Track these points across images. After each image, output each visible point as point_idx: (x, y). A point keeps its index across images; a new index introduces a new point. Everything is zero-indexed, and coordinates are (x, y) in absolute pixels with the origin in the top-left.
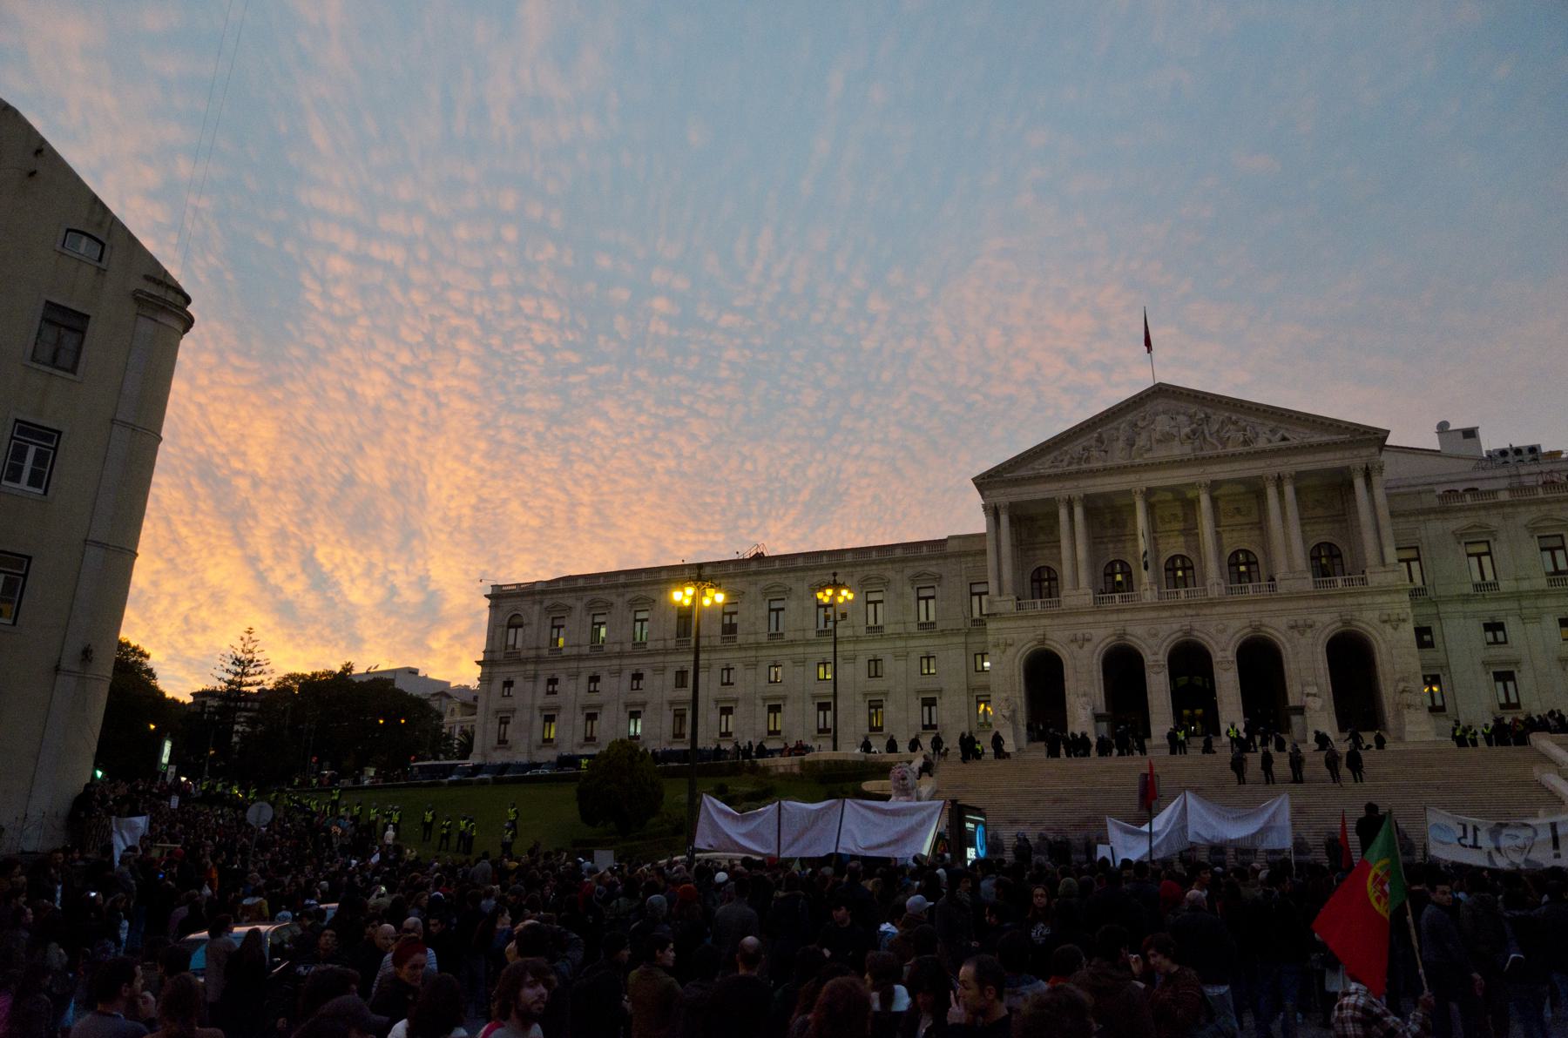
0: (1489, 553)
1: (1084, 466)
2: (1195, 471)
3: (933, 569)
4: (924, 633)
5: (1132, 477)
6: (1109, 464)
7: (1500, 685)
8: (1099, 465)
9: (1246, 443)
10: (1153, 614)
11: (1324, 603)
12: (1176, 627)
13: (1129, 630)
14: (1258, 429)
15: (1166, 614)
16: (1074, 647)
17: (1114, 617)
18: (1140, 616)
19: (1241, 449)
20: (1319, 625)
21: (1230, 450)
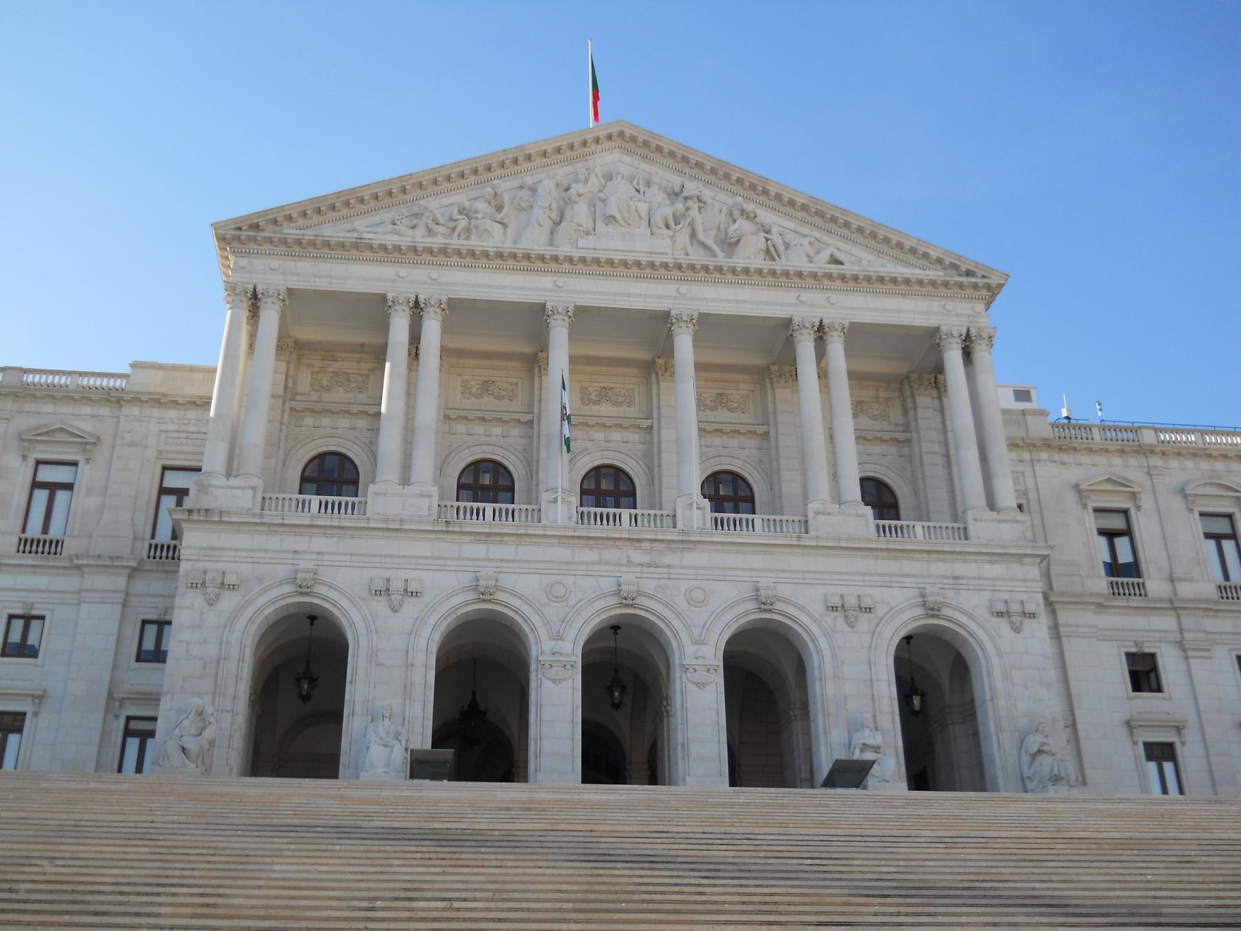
0: (1128, 532)
1: (455, 242)
2: (669, 289)
3: (85, 426)
4: (29, 560)
5: (546, 282)
6: (508, 246)
7: (1152, 767)
8: (489, 244)
9: (769, 254)
10: (560, 553)
11: (890, 566)
12: (607, 584)
13: (507, 580)
14: (790, 237)
15: (590, 555)
16: (380, 606)
17: (477, 550)
18: (531, 552)
19: (759, 262)
20: (880, 610)
21: (739, 261)
